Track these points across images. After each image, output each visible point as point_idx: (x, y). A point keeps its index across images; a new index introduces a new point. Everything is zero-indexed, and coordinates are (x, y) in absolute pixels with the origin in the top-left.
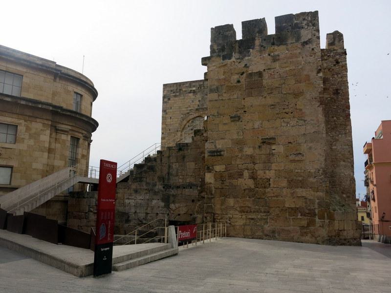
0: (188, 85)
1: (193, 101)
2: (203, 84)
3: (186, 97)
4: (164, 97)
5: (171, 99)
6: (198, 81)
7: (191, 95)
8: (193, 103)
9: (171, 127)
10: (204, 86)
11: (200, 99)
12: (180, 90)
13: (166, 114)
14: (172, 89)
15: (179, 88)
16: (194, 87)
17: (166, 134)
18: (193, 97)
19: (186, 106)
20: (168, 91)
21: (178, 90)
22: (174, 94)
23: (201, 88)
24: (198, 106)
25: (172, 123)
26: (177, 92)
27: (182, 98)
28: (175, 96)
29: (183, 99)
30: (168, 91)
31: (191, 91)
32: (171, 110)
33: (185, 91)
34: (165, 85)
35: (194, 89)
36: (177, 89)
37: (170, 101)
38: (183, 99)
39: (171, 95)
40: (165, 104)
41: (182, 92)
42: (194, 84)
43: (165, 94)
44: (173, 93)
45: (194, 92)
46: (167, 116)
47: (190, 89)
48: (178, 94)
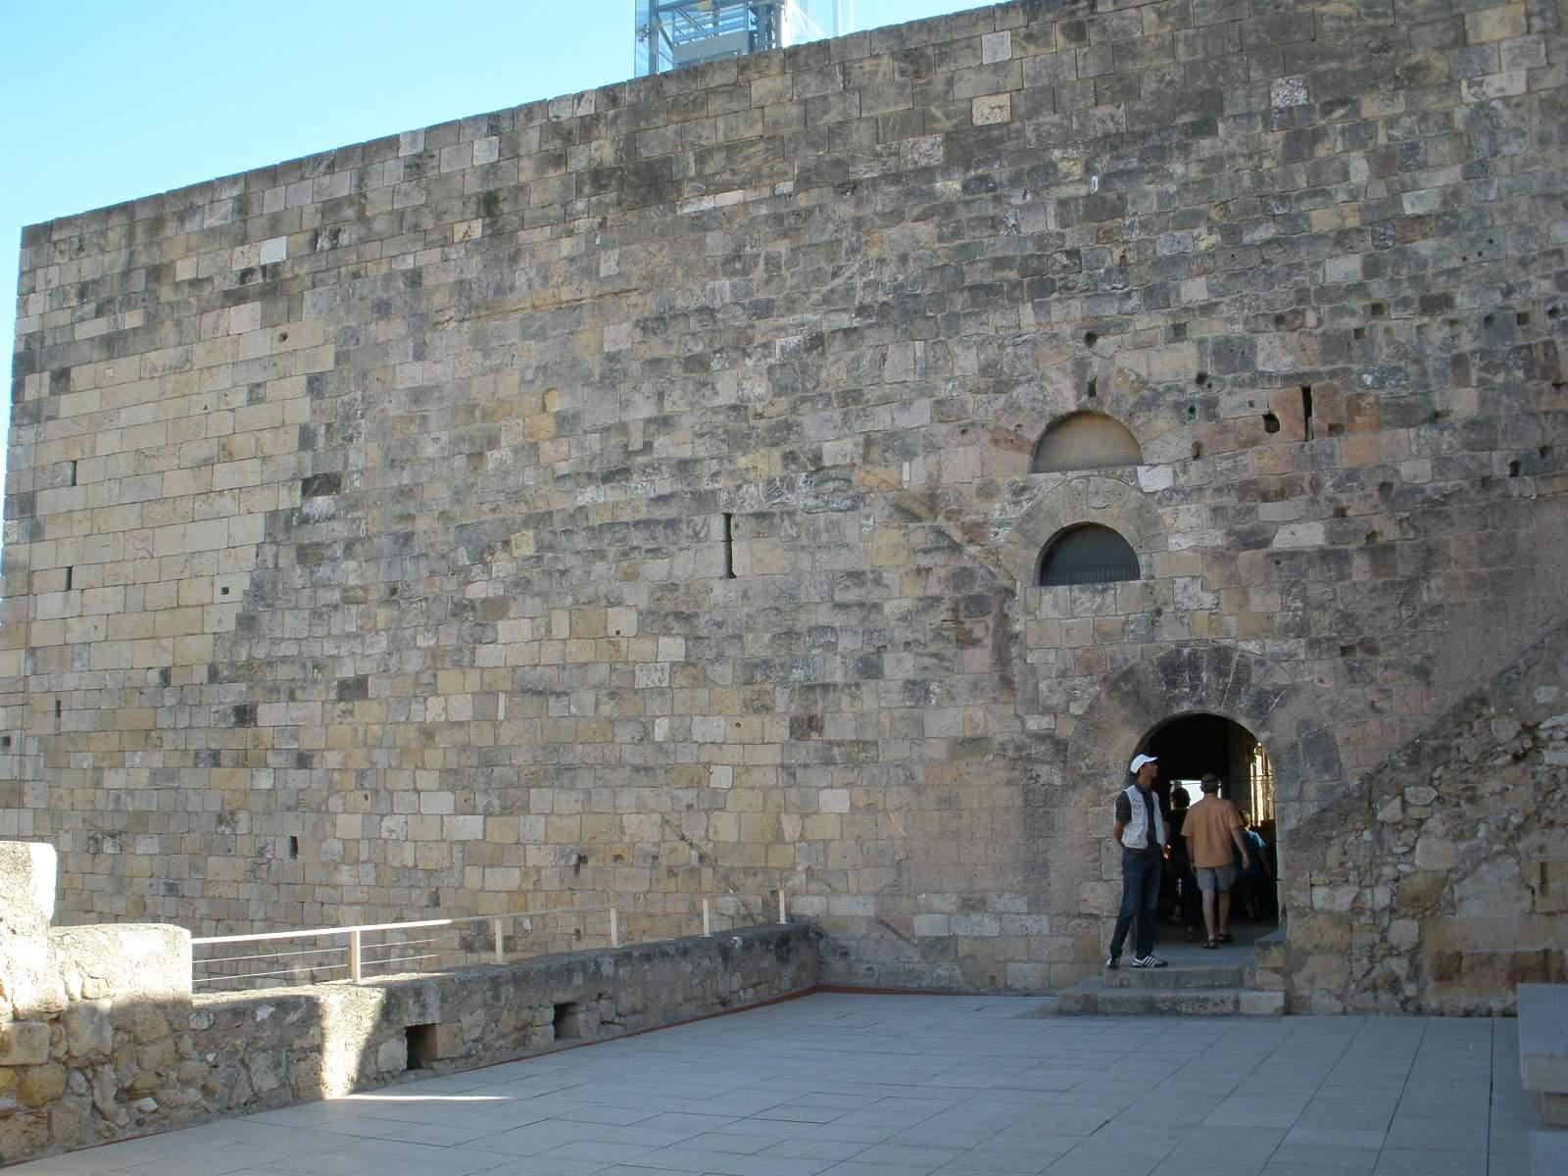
0: (218, 216)
1: (256, 394)
2: (359, 199)
3: (199, 350)
4: (24, 363)
5: (80, 376)
6: (317, 159)
7: (244, 317)
8: (262, 414)
9: (70, 680)
10: (362, 219)
11: (326, 362)
12: (156, 273)
13: (35, 533)
14: (89, 267)
15: (143, 259)
16: (274, 228)
17: (32, 747)
18: (261, 344)
19: (204, 451)
20: (58, 293)
21: (139, 281)
22: (100, 327)
23: (335, 235)
24: (306, 439)
25: (77, 631)
26: (128, 304)
27: (169, 356)
28: (112, 345)
29: (177, 369)
30: (58, 293)
31: (246, 274)
32: (74, 498)
33: (195, 283)
34: (36, 237)
35: (273, 251)
36: (126, 274)
37: (67, 404)
38: (177, 369)
39: (84, 331)
40: (28, 434)
41: (166, 294)
42: (273, 201)
43: (33, 326)
44: (99, 312)
45: (271, 287)
46: (43, 555)
47: (242, 259)
48: (133, 319)
